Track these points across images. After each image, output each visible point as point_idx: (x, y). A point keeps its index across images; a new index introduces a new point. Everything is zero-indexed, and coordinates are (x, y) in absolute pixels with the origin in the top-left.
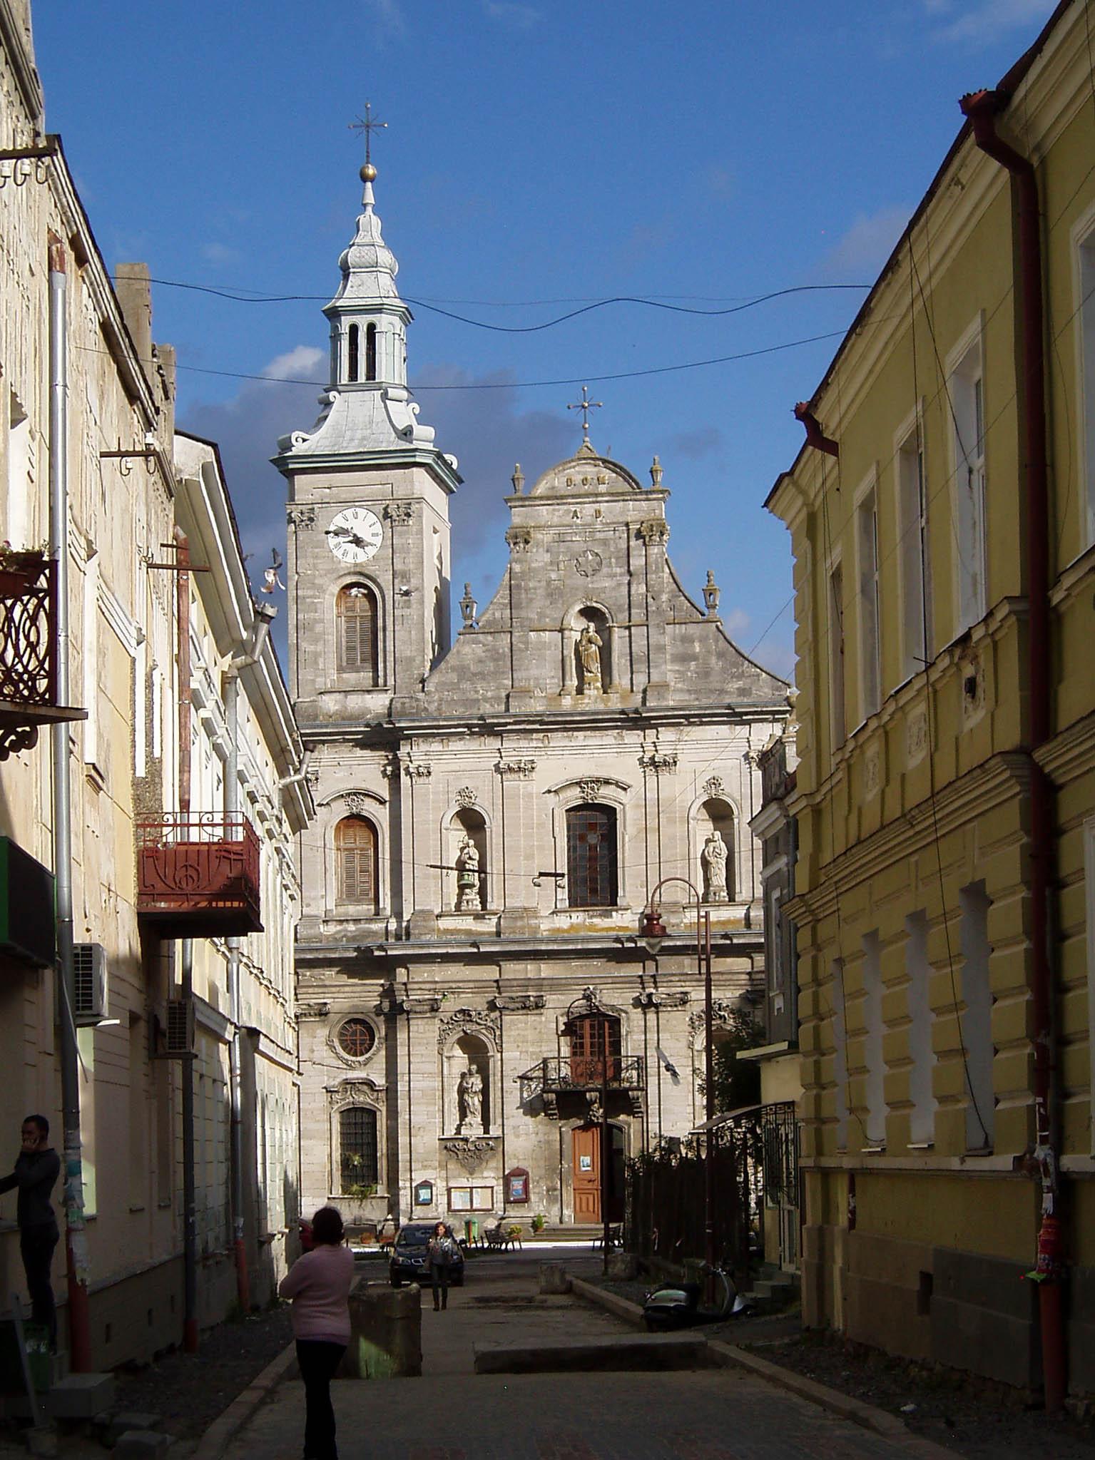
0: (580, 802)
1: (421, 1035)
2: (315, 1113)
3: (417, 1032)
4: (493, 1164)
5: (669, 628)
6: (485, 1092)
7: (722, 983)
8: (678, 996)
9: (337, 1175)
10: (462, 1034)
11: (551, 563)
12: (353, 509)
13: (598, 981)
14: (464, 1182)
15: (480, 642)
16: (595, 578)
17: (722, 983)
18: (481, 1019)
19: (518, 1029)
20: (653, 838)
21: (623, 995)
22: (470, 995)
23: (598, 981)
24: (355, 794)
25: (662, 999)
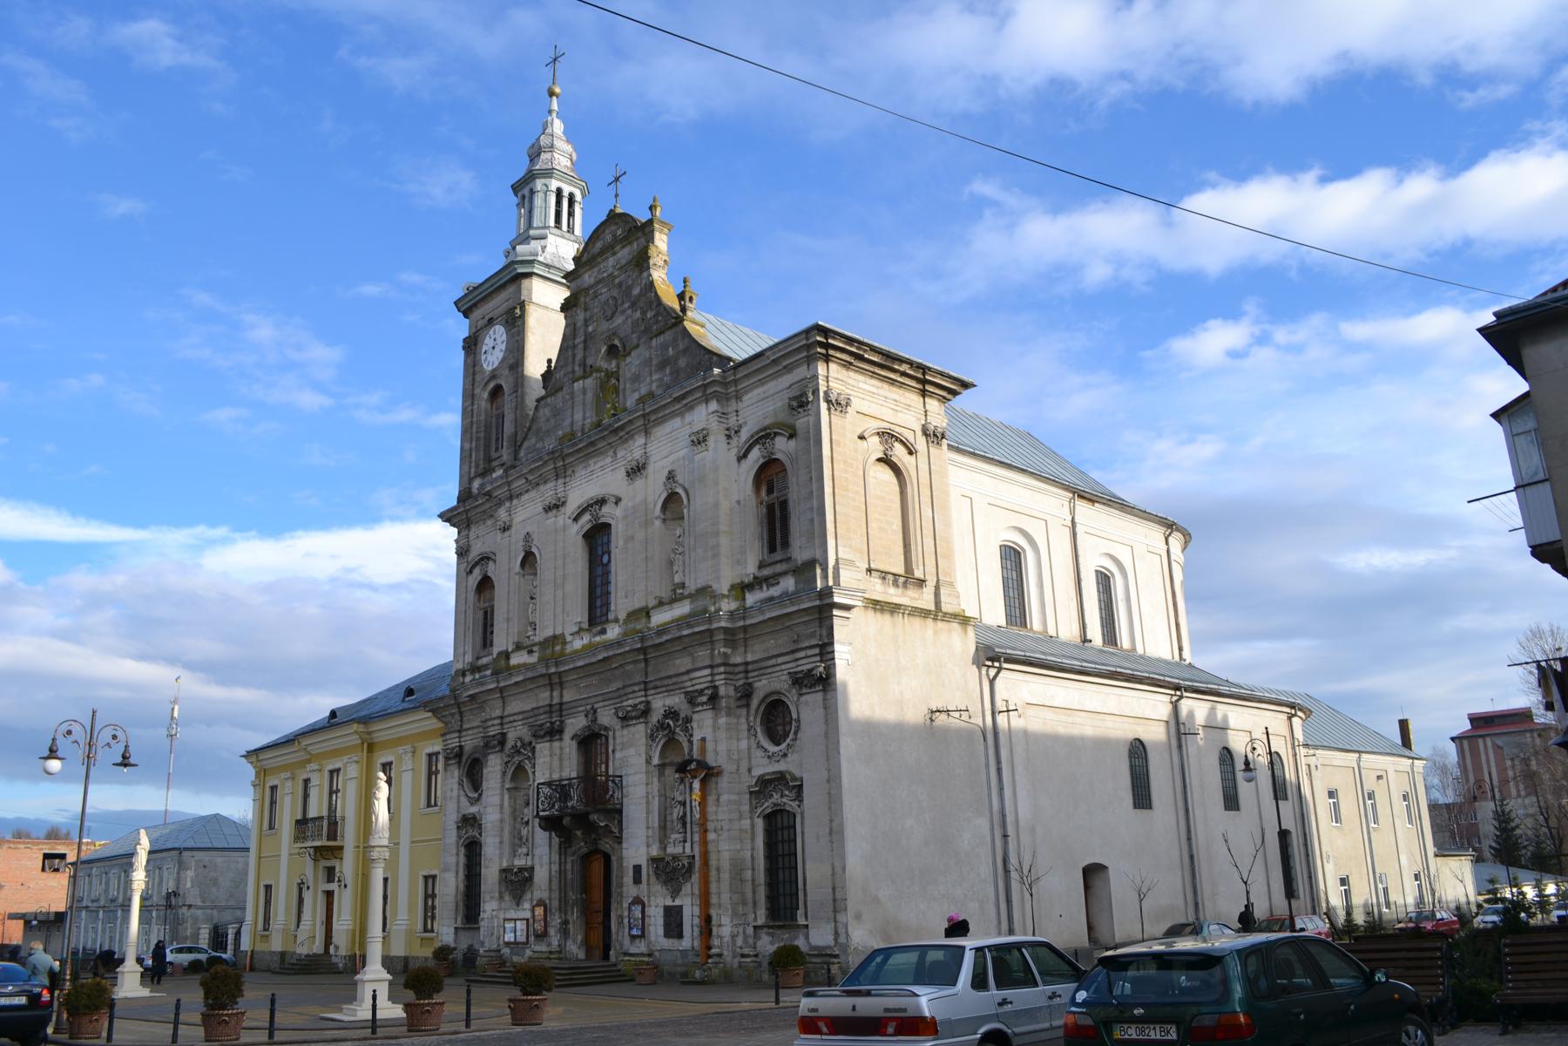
0: (589, 526)
4: (528, 896)
5: (654, 342)
6: (527, 823)
7: (672, 687)
9: (461, 904)
10: (515, 765)
11: (590, 318)
12: (493, 329)
13: (593, 700)
14: (512, 914)
15: (548, 405)
16: (613, 319)
17: (672, 687)
18: (525, 749)
19: (544, 756)
22: (520, 727)
23: (593, 700)
24: (482, 559)
25: (628, 712)
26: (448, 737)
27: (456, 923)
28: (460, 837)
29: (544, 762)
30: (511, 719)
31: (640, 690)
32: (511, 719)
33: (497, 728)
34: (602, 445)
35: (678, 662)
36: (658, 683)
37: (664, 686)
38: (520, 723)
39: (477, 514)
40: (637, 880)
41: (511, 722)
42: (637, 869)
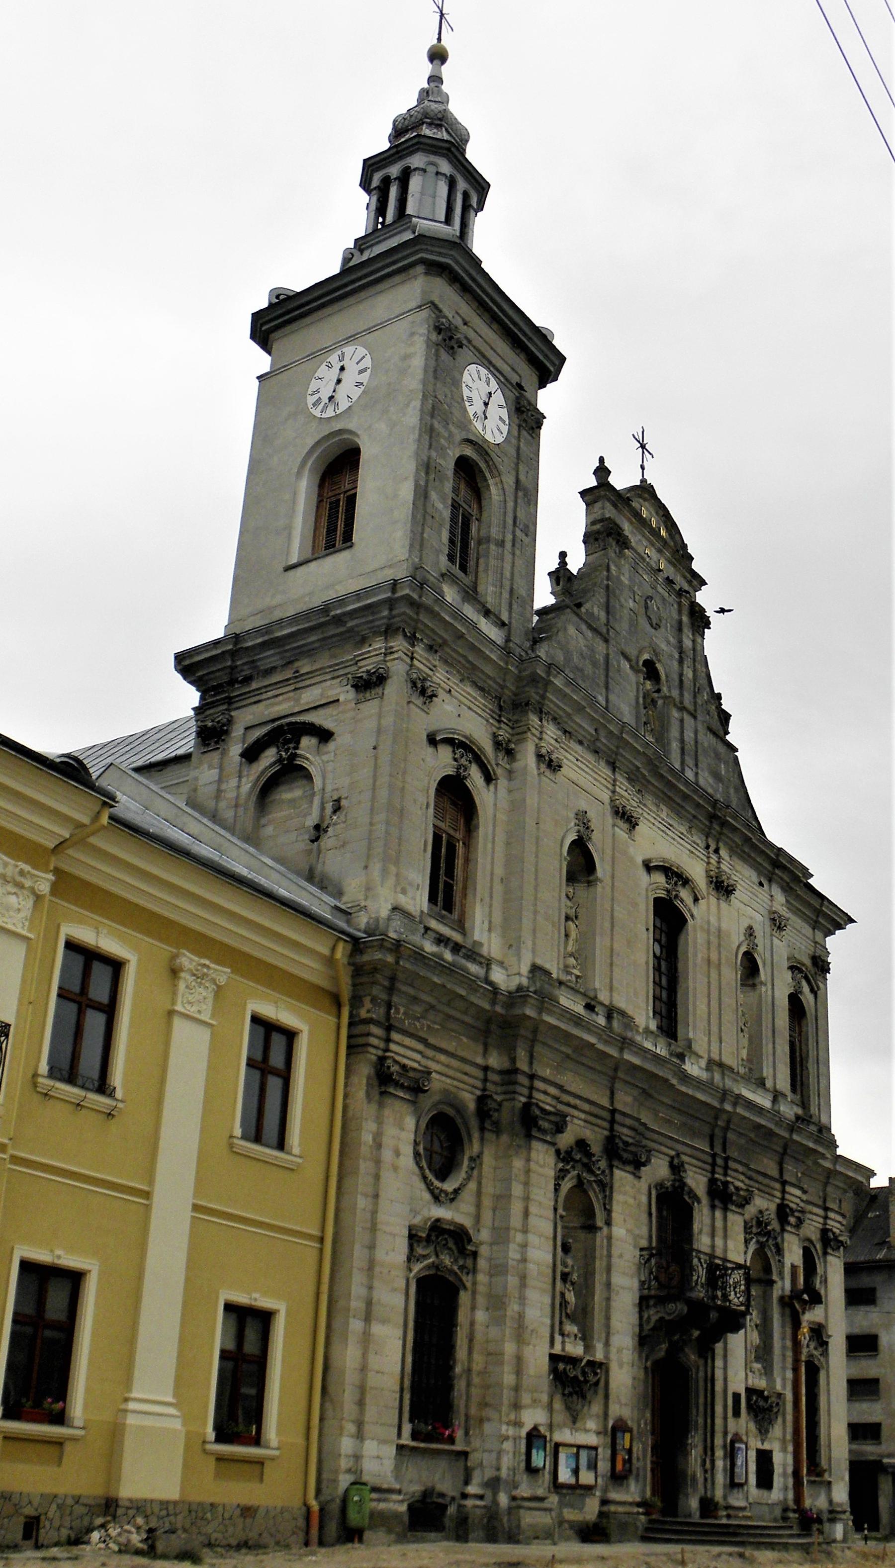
1: (541, 1170)
2: (393, 1273)
3: (537, 1163)
4: (596, 1408)
8: (742, 1193)
20: (714, 975)
21: (696, 1176)
22: (582, 1123)
26: (395, 1036)
27: (399, 1435)
28: (411, 1257)
29: (626, 1202)
30: (573, 1101)
31: (742, 1173)
32: (573, 1101)
33: (549, 1100)
34: (691, 810)
35: (765, 1160)
36: (754, 1175)
37: (757, 1181)
38: (583, 1116)
39: (464, 657)
40: (737, 1413)
41: (568, 1105)
42: (737, 1397)
